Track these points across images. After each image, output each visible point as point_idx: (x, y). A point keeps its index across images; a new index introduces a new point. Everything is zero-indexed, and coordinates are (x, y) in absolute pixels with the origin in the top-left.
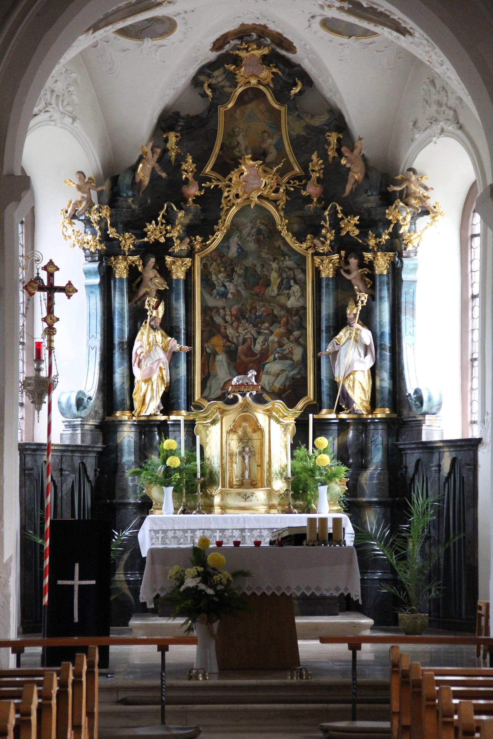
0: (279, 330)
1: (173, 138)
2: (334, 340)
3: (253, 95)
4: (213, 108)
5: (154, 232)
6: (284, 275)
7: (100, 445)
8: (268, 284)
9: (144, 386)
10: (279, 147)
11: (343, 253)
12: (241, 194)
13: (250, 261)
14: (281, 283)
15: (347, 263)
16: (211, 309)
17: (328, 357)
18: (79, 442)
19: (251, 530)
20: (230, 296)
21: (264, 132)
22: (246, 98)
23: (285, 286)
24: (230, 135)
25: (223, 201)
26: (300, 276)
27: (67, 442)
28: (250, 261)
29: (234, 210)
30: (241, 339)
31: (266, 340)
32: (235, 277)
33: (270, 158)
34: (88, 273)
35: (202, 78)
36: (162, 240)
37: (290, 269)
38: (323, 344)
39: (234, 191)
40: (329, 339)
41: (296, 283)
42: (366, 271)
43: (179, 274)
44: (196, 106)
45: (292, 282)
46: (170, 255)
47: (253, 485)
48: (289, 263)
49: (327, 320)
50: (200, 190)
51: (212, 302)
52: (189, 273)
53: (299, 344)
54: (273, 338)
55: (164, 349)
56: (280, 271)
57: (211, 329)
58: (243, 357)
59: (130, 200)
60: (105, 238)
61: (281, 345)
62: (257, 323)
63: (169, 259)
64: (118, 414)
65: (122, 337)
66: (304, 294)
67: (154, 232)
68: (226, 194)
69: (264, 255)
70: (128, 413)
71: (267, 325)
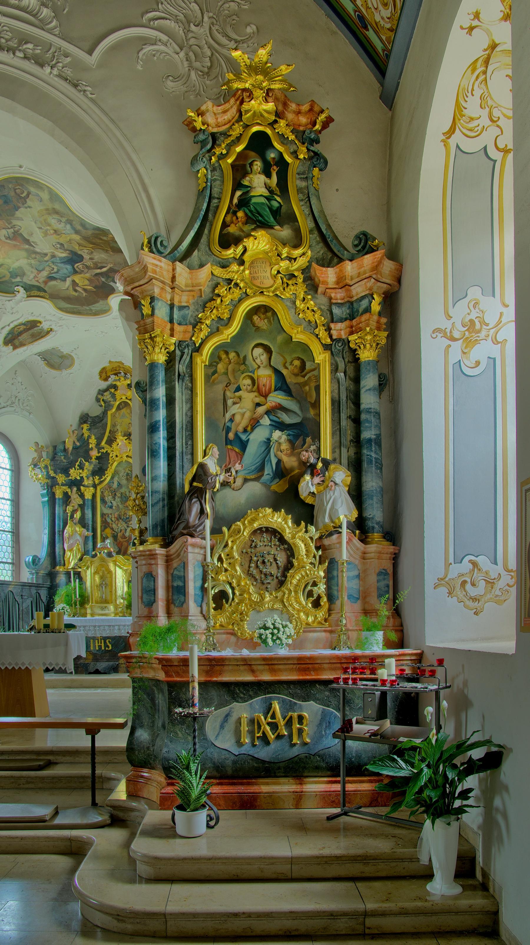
1: (85, 426)
4: (105, 413)
5: (74, 474)
7: (49, 583)
13: (123, 490)
18: (35, 582)
19: (99, 626)
20: (114, 508)
22: (121, 407)
24: (114, 425)
27: (30, 581)
28: (123, 490)
29: (115, 464)
32: (116, 498)
34: (43, 496)
35: (100, 396)
36: (78, 478)
39: (115, 454)
43: (88, 496)
44: (96, 411)
46: (84, 486)
47: (106, 602)
50: (99, 453)
51: (106, 511)
52: (94, 496)
55: (80, 535)
57: (105, 525)
58: (120, 539)
59: (63, 457)
60: (49, 477)
63: (82, 488)
64: (58, 568)
65: (59, 528)
67: (74, 474)
68: (111, 455)
70: (62, 567)
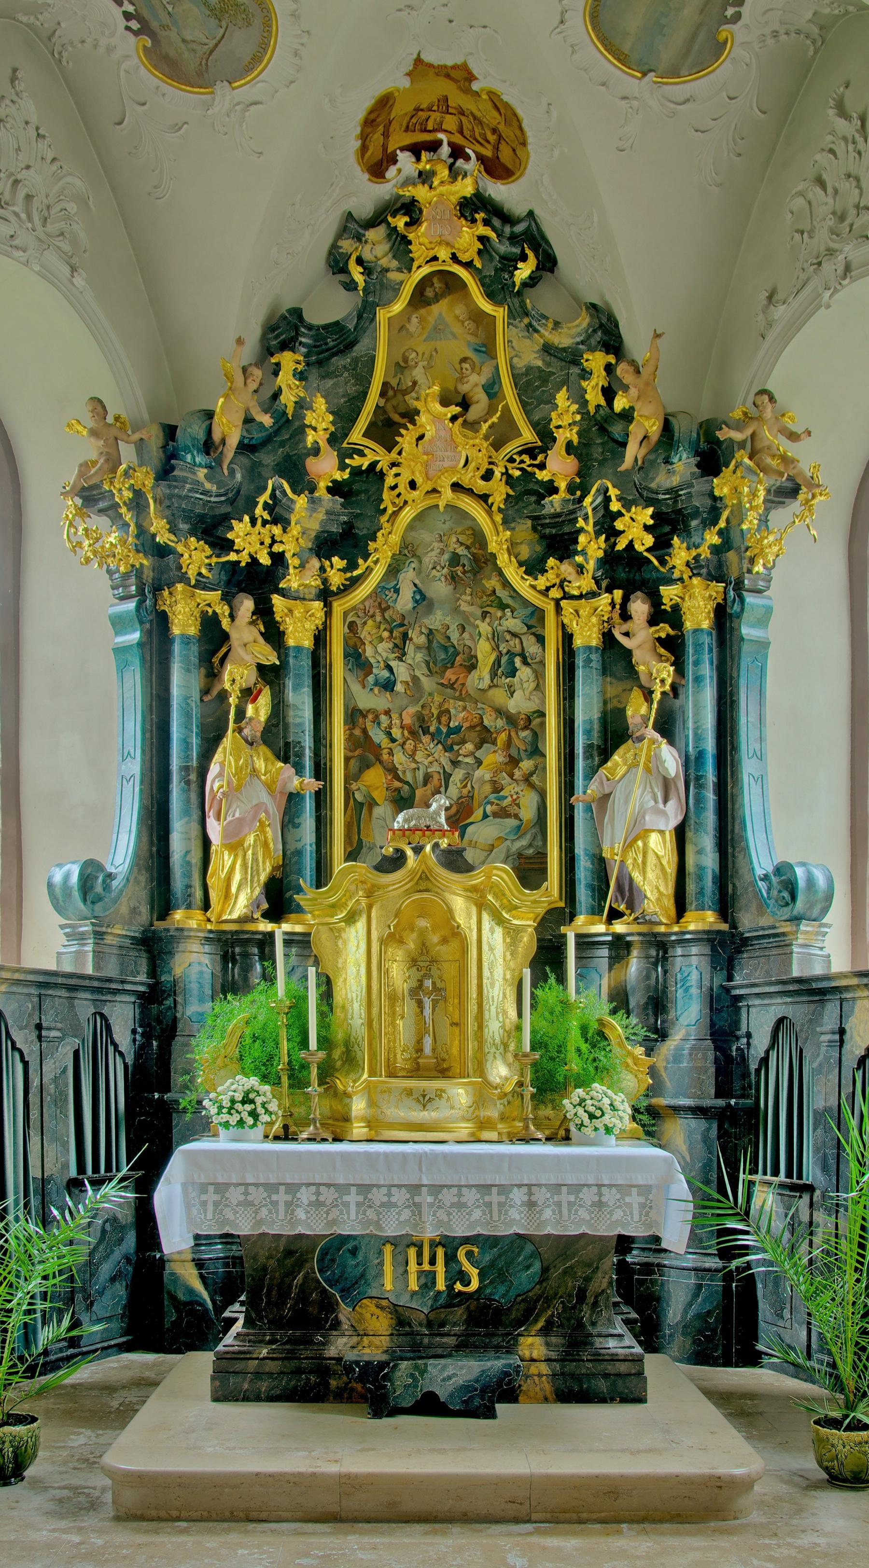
0: (493, 757)
2: (602, 771)
3: (441, 285)
4: (366, 313)
6: (503, 648)
8: (472, 666)
9: (228, 859)
10: (492, 389)
11: (618, 594)
12: (419, 481)
13: (436, 620)
14: (497, 663)
15: (625, 616)
16: (363, 714)
17: (589, 809)
20: (399, 687)
21: (464, 360)
22: (429, 293)
23: (504, 669)
24: (401, 366)
25: (386, 495)
26: (532, 648)
28: (436, 620)
29: (407, 515)
30: (420, 775)
31: (468, 777)
32: (410, 649)
33: (474, 413)
37: (514, 635)
38: (579, 781)
40: (592, 772)
41: (525, 662)
42: (664, 630)
45: (518, 661)
48: (512, 623)
49: (588, 733)
51: (366, 700)
53: (532, 786)
54: (483, 774)
55: (269, 787)
56: (496, 638)
57: (364, 753)
61: (497, 789)
62: (449, 739)
66: (539, 687)
68: (390, 481)
69: (464, 607)
70: (198, 914)
71: (469, 746)
